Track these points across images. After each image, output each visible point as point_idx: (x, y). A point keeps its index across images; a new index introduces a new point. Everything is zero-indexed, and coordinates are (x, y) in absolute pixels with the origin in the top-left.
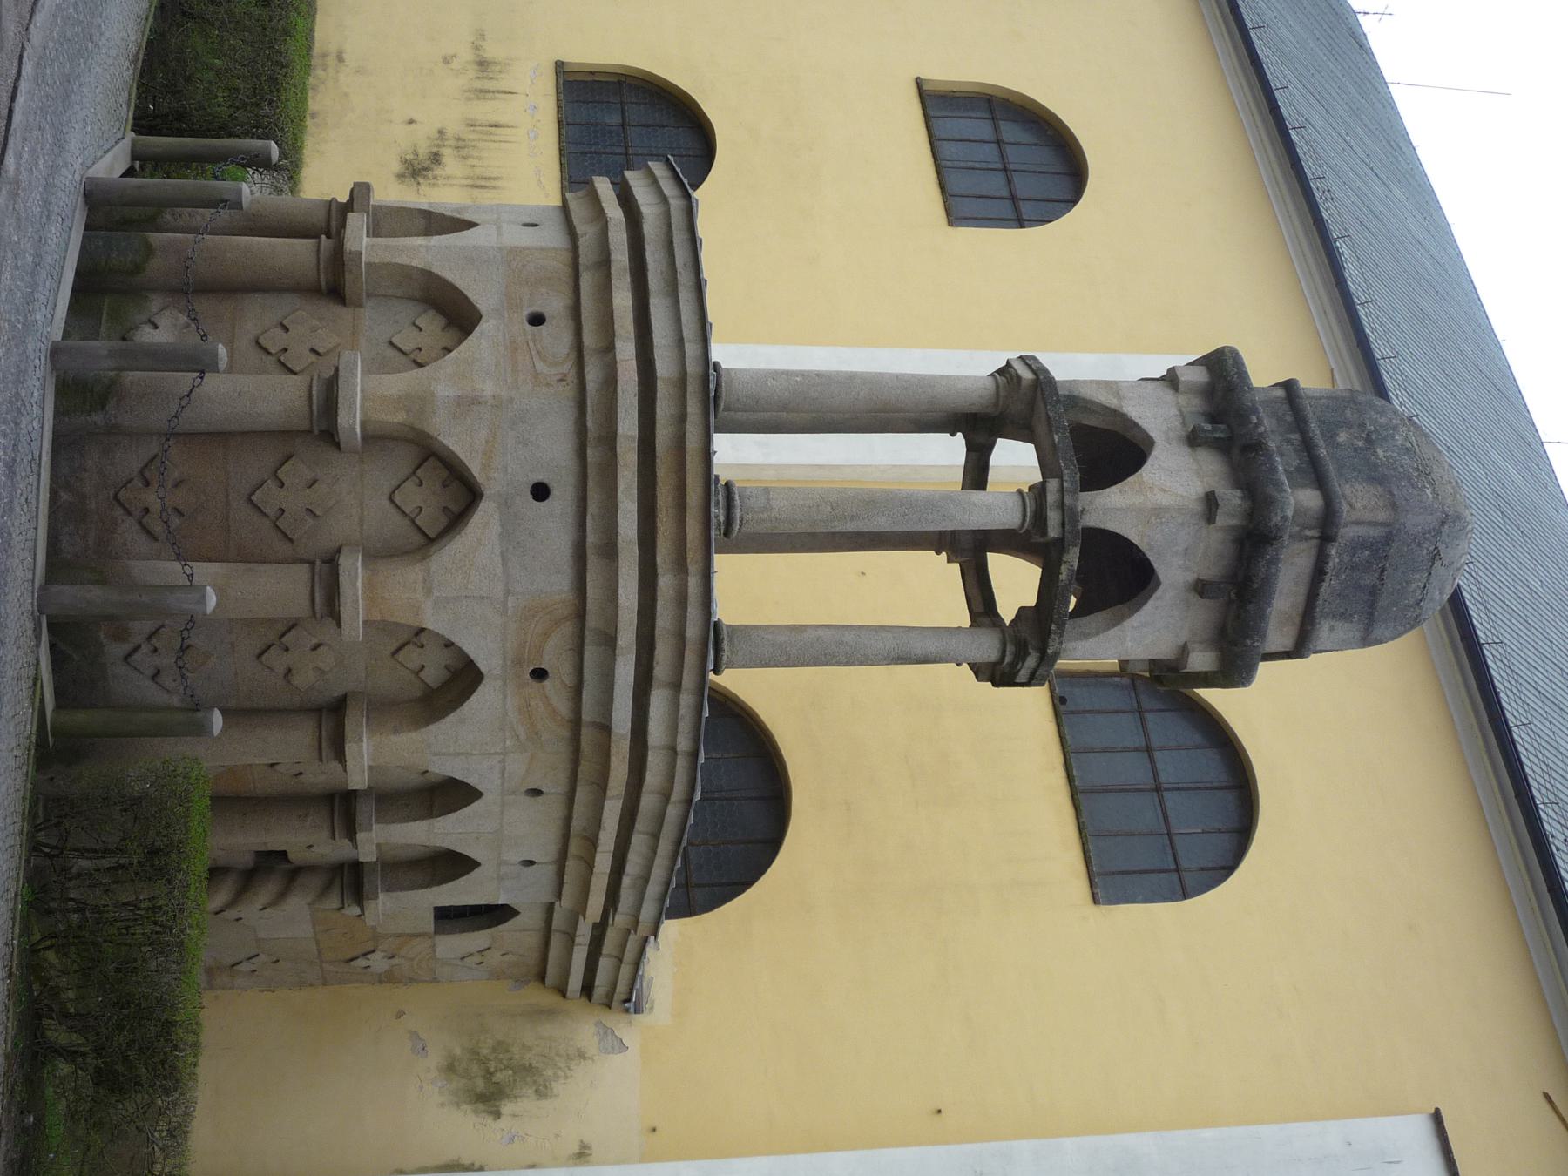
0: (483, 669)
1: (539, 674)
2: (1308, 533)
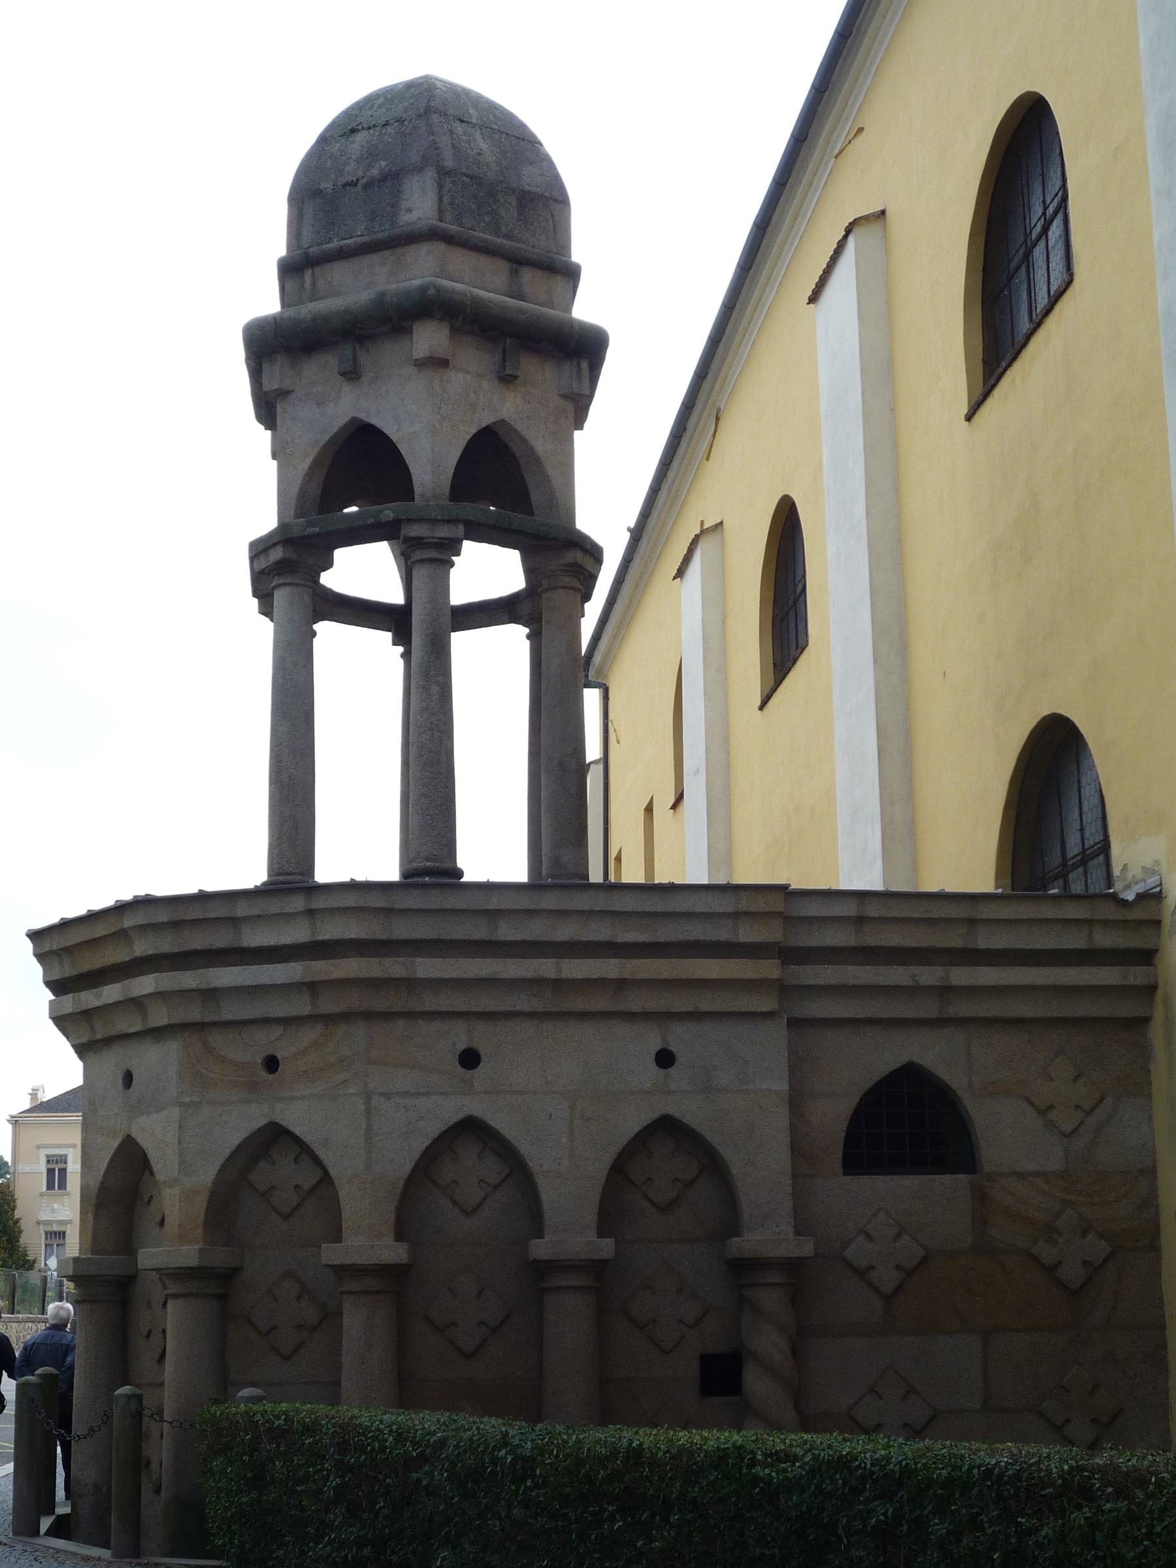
0: (264, 1121)
1: (272, 1064)
2: (308, 284)
